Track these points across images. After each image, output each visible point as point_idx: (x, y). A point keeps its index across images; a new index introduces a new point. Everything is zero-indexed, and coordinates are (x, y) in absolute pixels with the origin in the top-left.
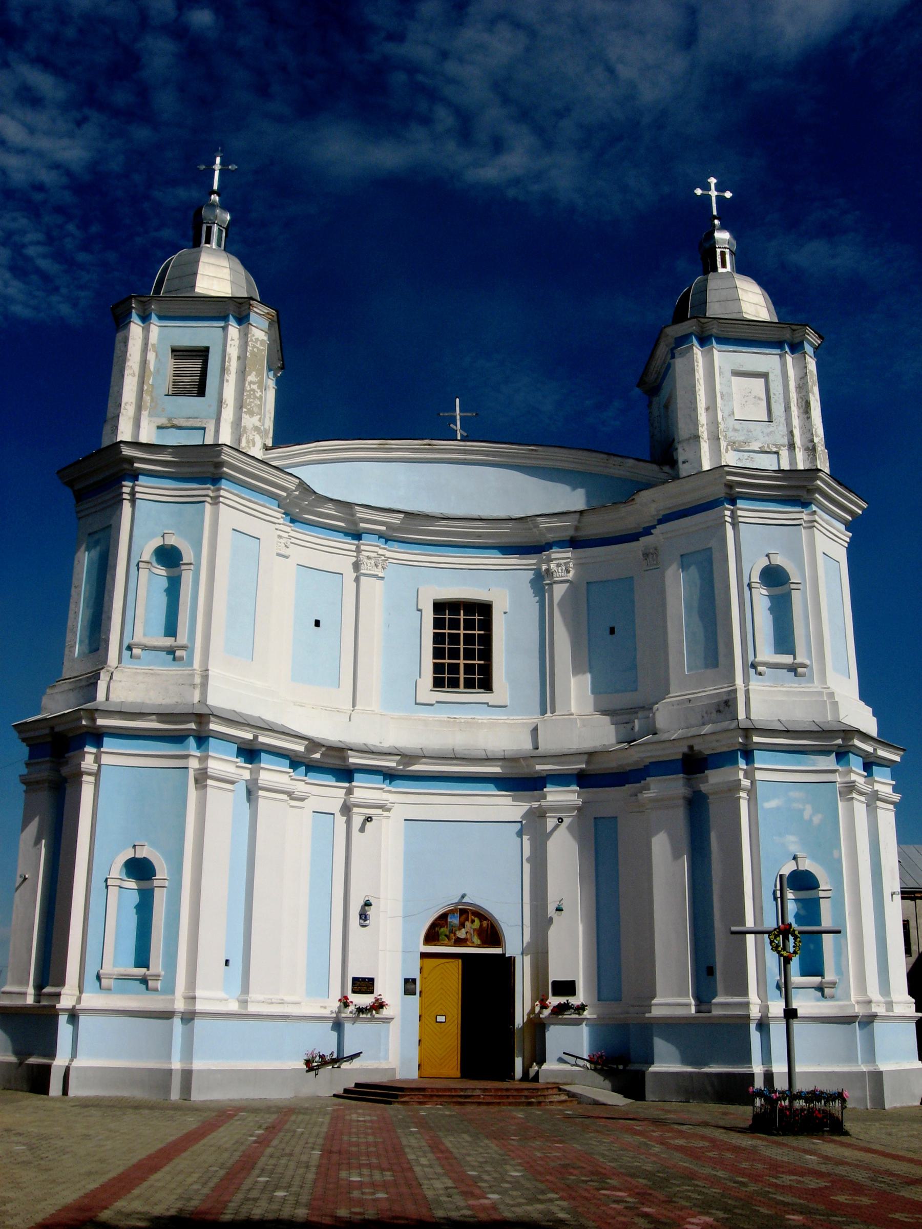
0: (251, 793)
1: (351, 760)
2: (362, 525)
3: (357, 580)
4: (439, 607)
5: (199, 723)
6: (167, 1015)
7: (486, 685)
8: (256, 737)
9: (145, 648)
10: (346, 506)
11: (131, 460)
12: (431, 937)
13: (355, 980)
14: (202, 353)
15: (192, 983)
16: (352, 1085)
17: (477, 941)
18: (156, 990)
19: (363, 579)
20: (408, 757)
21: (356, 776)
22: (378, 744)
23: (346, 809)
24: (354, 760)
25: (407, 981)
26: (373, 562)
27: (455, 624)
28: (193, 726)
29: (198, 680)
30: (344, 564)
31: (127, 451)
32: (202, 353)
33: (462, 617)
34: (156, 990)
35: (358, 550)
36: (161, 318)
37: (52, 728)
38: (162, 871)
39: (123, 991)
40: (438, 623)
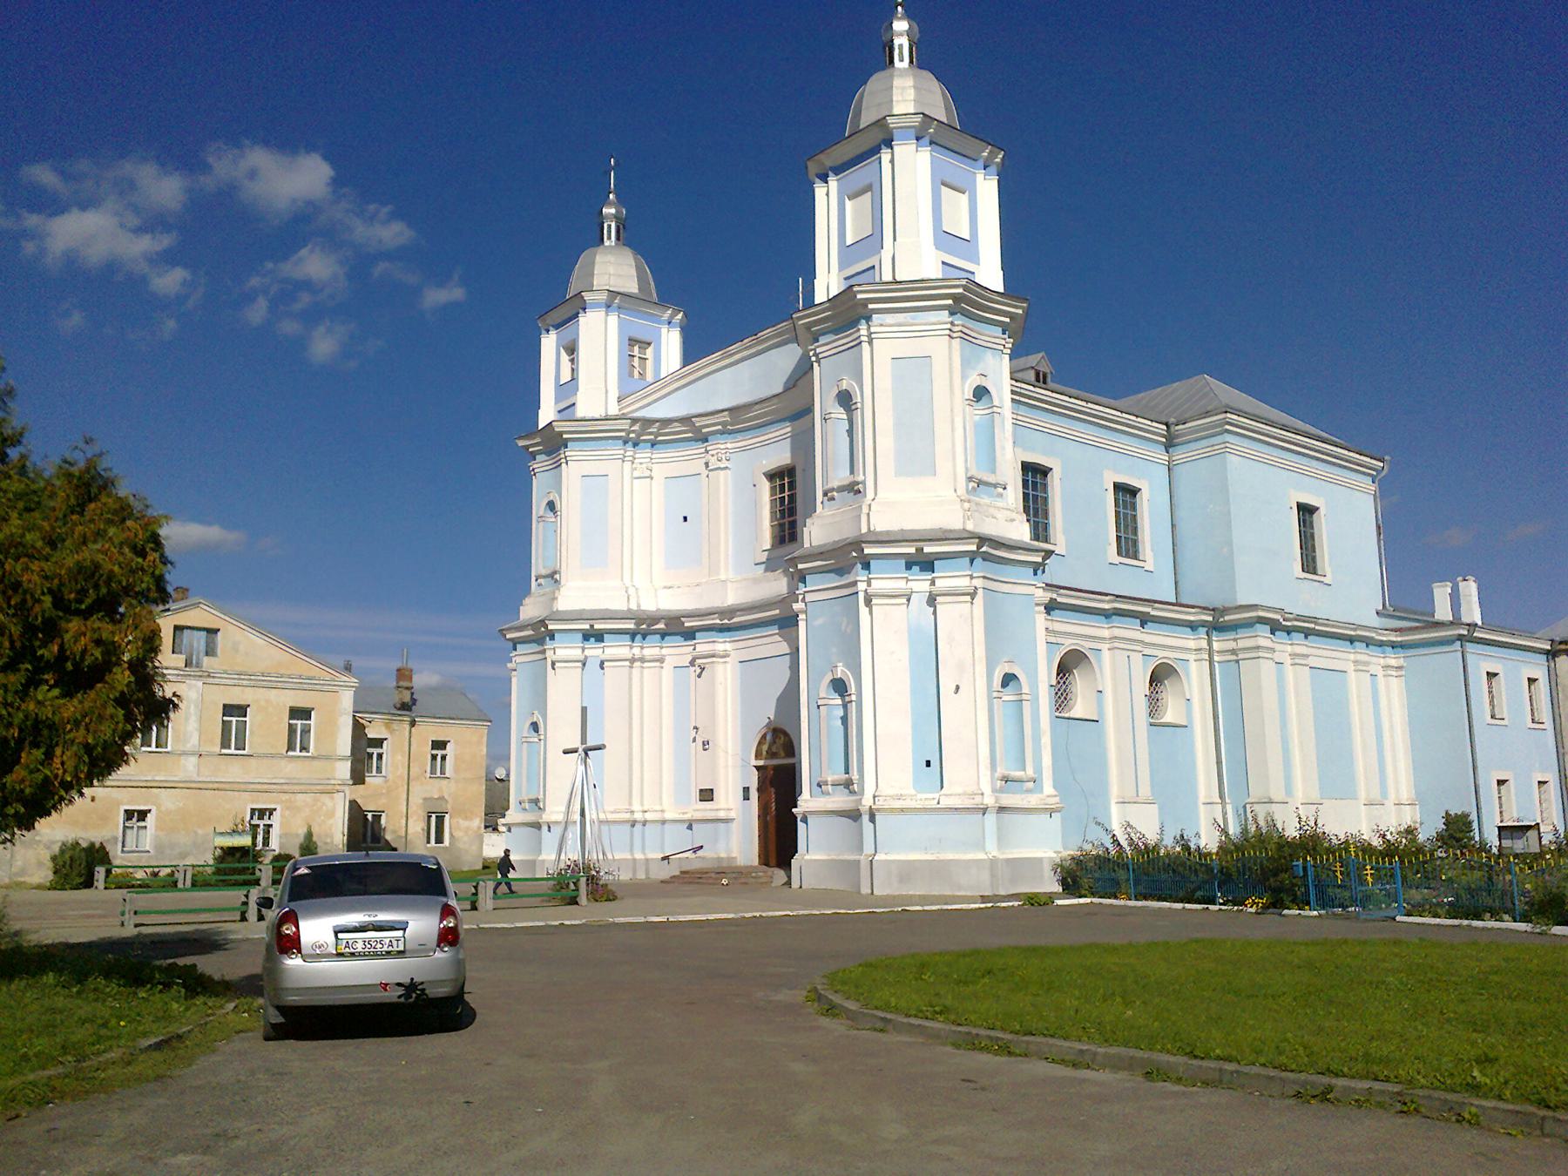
1: (686, 625)
2: (704, 430)
8: (592, 626)
10: (686, 420)
11: (527, 447)
12: (758, 756)
17: (783, 754)
20: (730, 612)
21: (697, 634)
22: (720, 605)
26: (715, 457)
28: (531, 632)
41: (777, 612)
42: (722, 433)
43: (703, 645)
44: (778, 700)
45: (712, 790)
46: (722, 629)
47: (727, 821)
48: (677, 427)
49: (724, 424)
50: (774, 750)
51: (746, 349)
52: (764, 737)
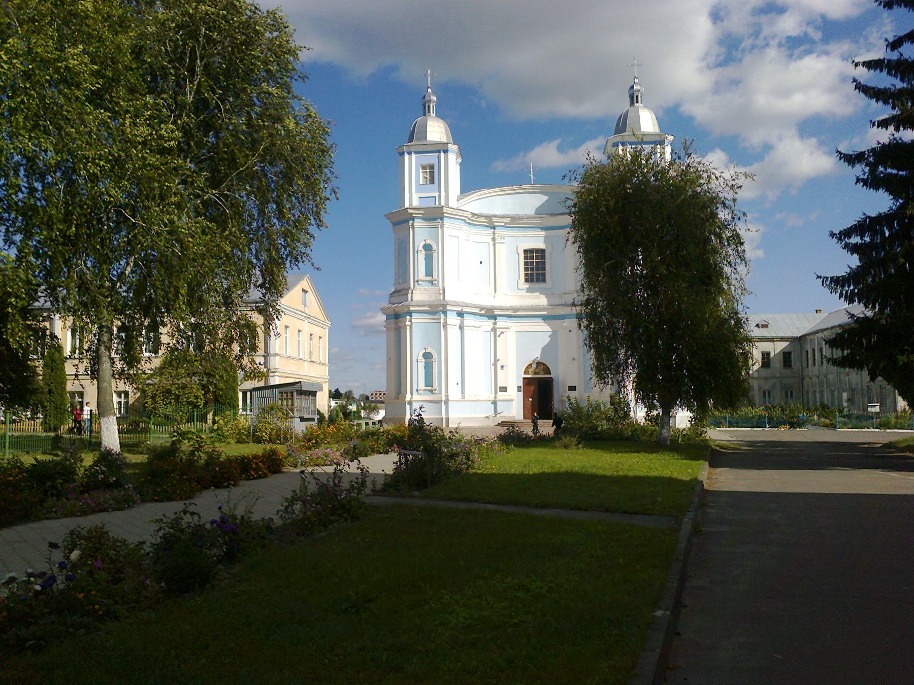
0: (461, 328)
1: (495, 313)
2: (495, 224)
3: (494, 245)
4: (526, 251)
5: (443, 308)
6: (439, 402)
7: (544, 280)
9: (423, 281)
10: (488, 217)
12: (526, 372)
13: (500, 388)
14: (432, 167)
15: (447, 391)
16: (500, 422)
17: (542, 373)
18: (436, 394)
19: (497, 245)
20: (515, 309)
23: (494, 330)
24: (496, 312)
25: (518, 387)
27: (532, 258)
29: (441, 291)
30: (489, 239)
31: (410, 211)
32: (432, 167)
33: (534, 255)
34: (436, 394)
35: (494, 233)
36: (416, 153)
37: (394, 310)
38: (435, 356)
39: (426, 395)
40: (526, 258)
41: (546, 313)
42: (502, 226)
43: (501, 322)
44: (543, 349)
45: (506, 387)
46: (509, 316)
47: (512, 401)
48: (483, 219)
49: (505, 223)
50: (537, 371)
51: (514, 190)
52: (530, 365)
